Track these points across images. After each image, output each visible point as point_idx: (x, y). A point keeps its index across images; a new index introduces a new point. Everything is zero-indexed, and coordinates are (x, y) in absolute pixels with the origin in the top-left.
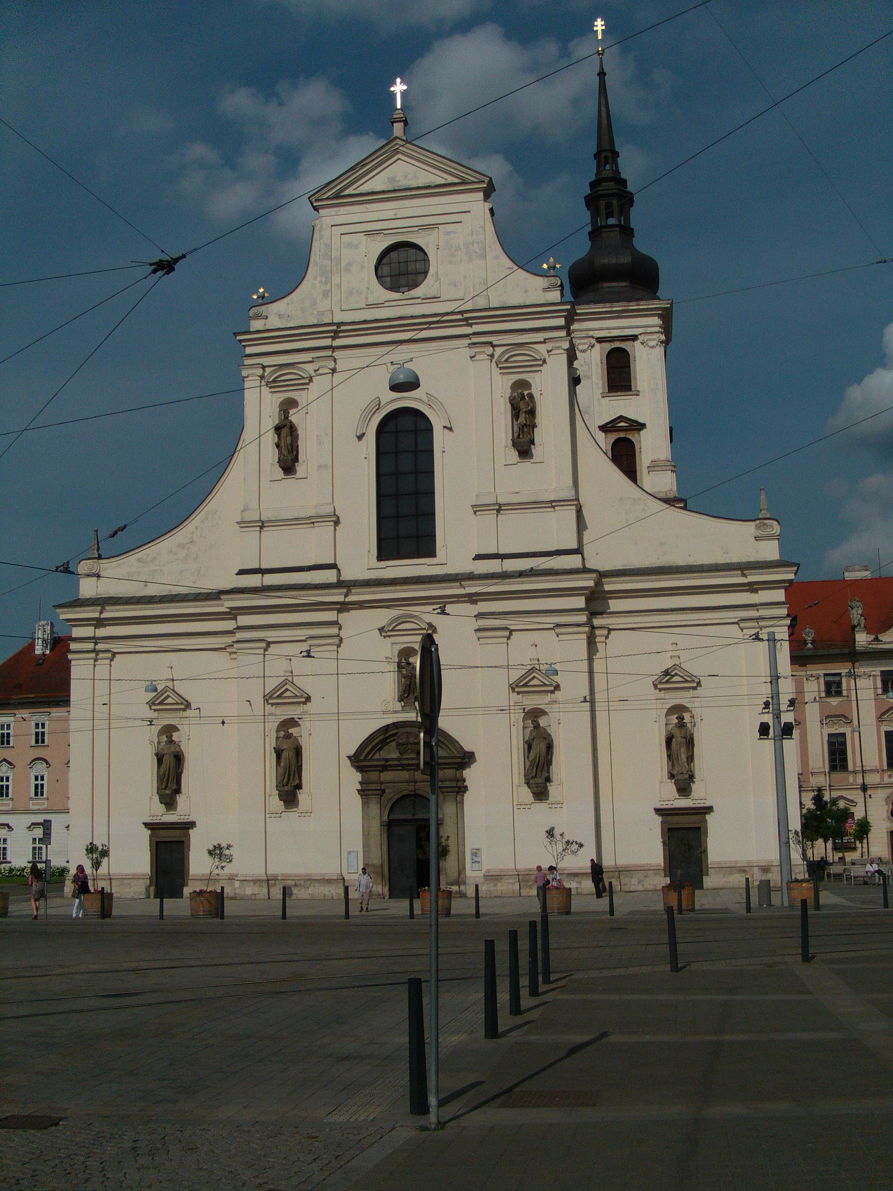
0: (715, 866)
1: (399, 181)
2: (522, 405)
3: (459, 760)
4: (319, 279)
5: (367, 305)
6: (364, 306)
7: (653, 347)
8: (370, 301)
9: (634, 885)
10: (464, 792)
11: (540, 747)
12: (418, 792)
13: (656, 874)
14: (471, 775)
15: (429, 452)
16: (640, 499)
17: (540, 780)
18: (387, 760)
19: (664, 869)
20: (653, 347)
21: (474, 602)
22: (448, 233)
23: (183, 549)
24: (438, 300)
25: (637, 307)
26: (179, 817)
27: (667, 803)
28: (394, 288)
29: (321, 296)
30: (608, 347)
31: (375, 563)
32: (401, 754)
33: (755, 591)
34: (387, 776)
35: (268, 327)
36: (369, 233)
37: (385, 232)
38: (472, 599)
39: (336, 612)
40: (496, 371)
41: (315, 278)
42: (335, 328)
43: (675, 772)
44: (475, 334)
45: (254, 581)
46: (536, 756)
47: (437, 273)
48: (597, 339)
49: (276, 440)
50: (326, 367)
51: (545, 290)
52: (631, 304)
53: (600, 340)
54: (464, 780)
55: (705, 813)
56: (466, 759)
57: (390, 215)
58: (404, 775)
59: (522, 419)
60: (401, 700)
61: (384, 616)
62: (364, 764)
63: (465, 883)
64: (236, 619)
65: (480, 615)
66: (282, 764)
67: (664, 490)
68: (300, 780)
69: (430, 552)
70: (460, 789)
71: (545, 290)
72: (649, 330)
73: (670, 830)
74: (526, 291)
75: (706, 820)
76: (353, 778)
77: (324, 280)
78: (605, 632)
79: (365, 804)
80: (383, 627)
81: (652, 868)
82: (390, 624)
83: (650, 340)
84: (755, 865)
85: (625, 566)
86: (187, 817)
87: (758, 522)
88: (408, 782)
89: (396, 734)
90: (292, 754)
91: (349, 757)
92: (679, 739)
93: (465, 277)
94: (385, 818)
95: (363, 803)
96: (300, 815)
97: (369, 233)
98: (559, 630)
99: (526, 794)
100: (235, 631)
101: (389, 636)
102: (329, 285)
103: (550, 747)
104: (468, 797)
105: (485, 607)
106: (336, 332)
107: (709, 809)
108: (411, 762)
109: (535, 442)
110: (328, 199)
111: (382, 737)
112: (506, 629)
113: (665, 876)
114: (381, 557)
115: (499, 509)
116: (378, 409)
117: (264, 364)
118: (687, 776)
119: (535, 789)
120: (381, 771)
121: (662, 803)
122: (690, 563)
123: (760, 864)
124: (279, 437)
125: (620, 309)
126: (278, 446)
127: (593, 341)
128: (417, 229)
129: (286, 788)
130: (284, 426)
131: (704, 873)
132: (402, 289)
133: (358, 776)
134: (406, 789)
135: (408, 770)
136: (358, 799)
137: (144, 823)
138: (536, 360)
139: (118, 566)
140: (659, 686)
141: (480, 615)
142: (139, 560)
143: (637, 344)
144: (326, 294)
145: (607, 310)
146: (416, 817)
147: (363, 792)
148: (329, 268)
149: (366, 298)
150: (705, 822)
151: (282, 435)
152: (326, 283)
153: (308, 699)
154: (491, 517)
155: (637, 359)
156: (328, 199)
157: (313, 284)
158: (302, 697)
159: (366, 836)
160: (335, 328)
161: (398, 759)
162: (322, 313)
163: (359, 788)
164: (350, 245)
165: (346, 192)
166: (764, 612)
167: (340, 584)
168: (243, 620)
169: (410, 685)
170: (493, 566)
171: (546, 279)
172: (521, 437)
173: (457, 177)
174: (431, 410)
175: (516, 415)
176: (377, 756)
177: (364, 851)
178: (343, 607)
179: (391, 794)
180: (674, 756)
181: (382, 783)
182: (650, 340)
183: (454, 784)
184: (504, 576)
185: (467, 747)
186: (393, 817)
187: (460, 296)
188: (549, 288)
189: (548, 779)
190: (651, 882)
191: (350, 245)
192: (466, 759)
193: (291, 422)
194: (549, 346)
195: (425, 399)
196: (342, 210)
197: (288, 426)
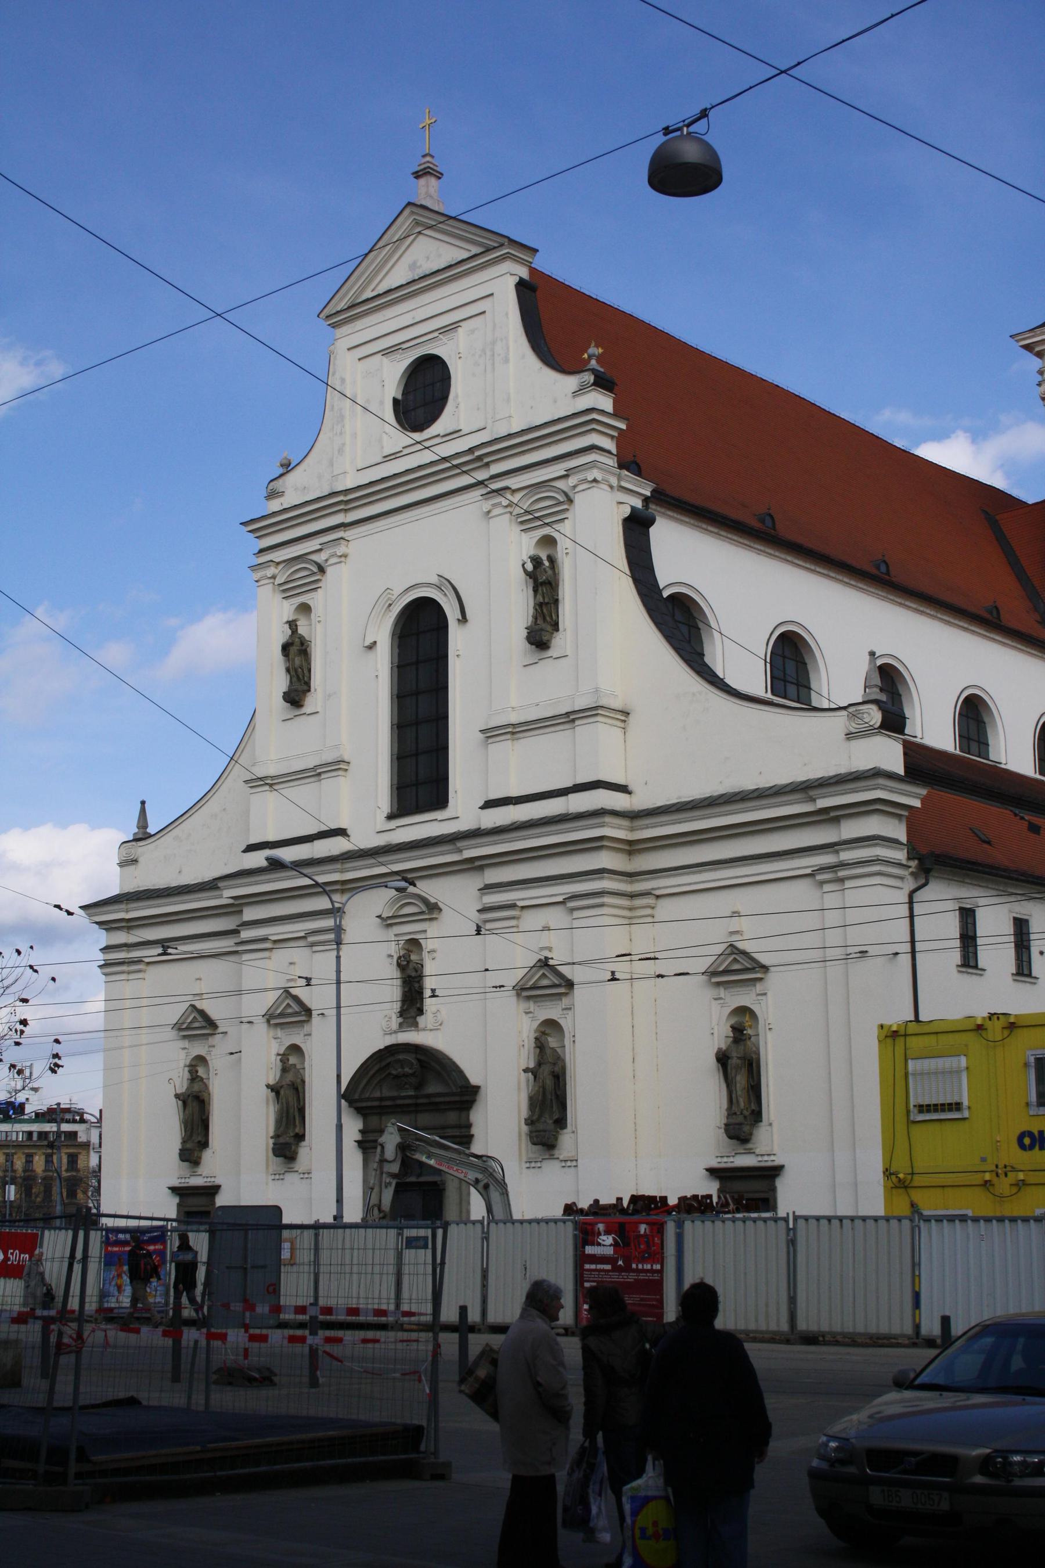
1: (421, 266)
5: (385, 457)
6: (380, 460)
21: (481, 868)
22: (473, 331)
26: (205, 1180)
27: (725, 1159)
33: (836, 820)
35: (286, 506)
36: (387, 352)
37: (404, 346)
38: (476, 865)
44: (493, 477)
45: (258, 859)
46: (538, 1091)
51: (576, 394)
54: (469, 1126)
64: (241, 912)
65: (488, 888)
71: (576, 394)
78: (649, 901)
85: (680, 798)
86: (213, 1179)
96: (302, 1176)
97: (387, 352)
98: (572, 904)
100: (239, 928)
105: (494, 876)
107: (775, 1171)
111: (376, 1068)
112: (512, 906)
116: (390, 605)
117: (277, 560)
119: (535, 1139)
128: (436, 334)
129: (281, 1140)
137: (169, 1188)
138: (560, 503)
141: (488, 888)
146: (422, 1179)
150: (773, 1190)
163: (359, 1137)
165: (369, 294)
166: (846, 856)
168: (250, 914)
169: (410, 989)
172: (538, 622)
173: (479, 244)
185: (474, 1080)
188: (582, 390)
194: (572, 481)
196: (359, 324)
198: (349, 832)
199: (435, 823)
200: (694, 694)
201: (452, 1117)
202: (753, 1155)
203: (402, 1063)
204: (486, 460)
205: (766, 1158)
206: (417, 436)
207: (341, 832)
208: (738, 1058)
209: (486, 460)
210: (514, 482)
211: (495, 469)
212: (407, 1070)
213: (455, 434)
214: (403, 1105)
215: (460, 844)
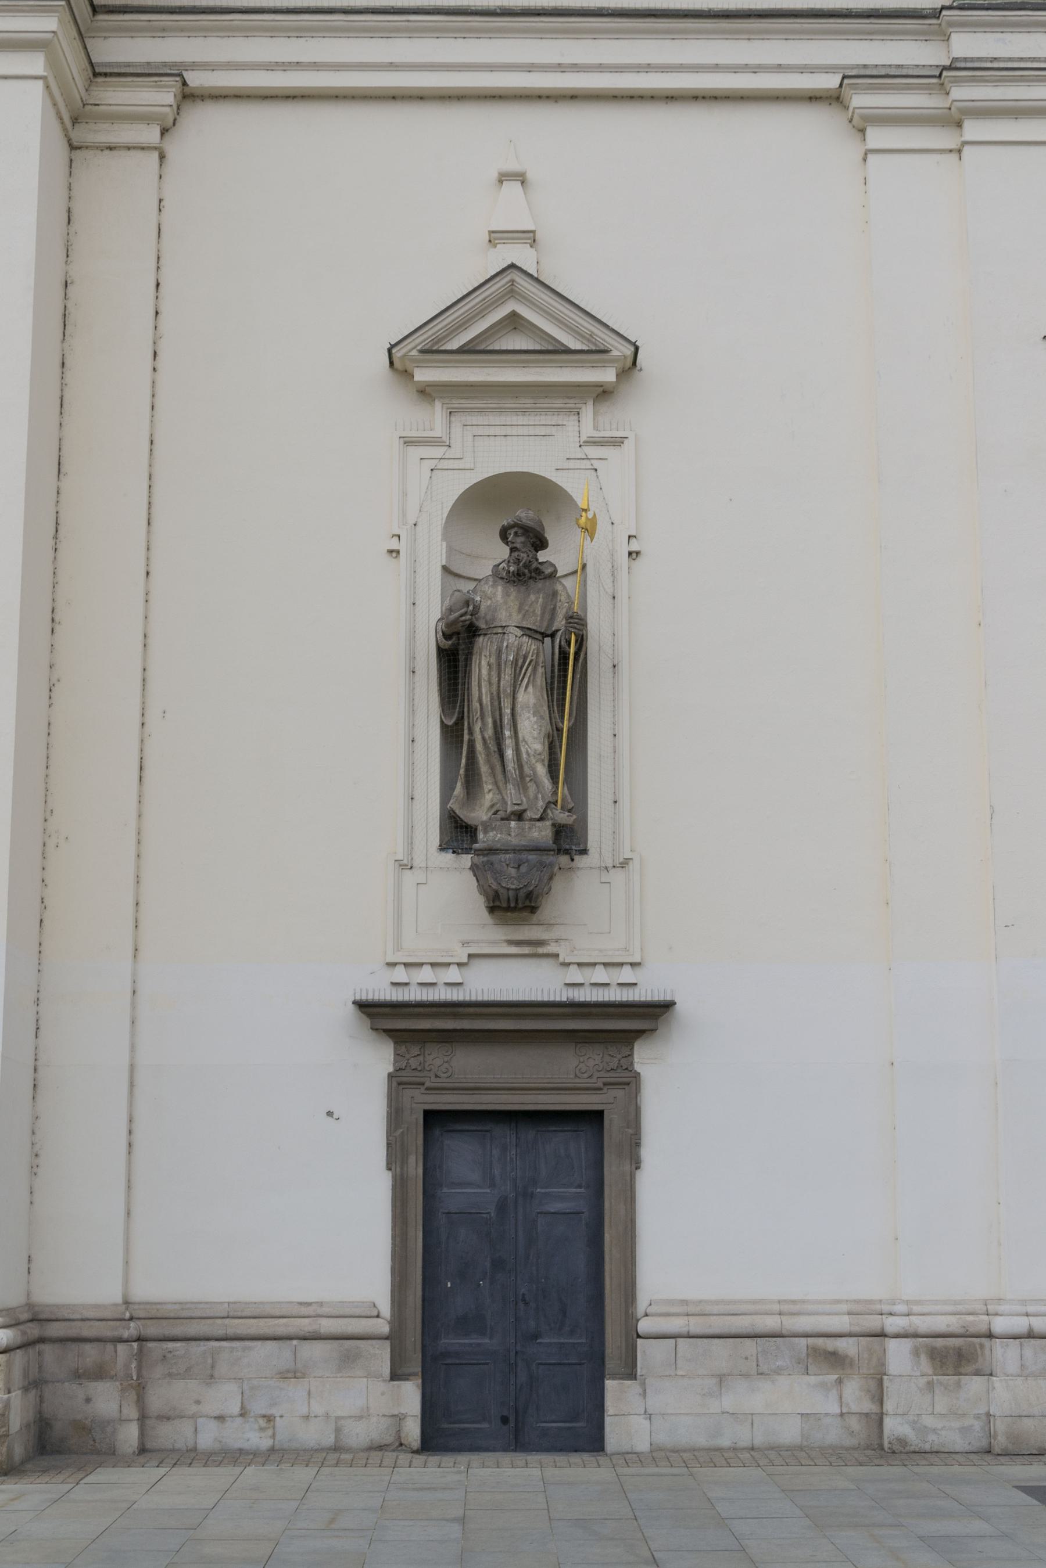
0: (676, 1325)
9: (220, 1418)
13: (347, 1361)
19: (395, 1337)
27: (426, 974)
43: (479, 814)
55: (630, 1037)
73: (433, 1118)
75: (637, 1076)
81: (327, 1326)
84: (893, 1324)
92: (513, 638)
113: (395, 1376)
118: (542, 833)
121: (400, 975)
123: (922, 1324)
131: (610, 1365)
140: (423, 375)
180: (481, 731)
190: (317, 1408)
202: (546, 965)
205: (600, 975)
208: (529, 632)
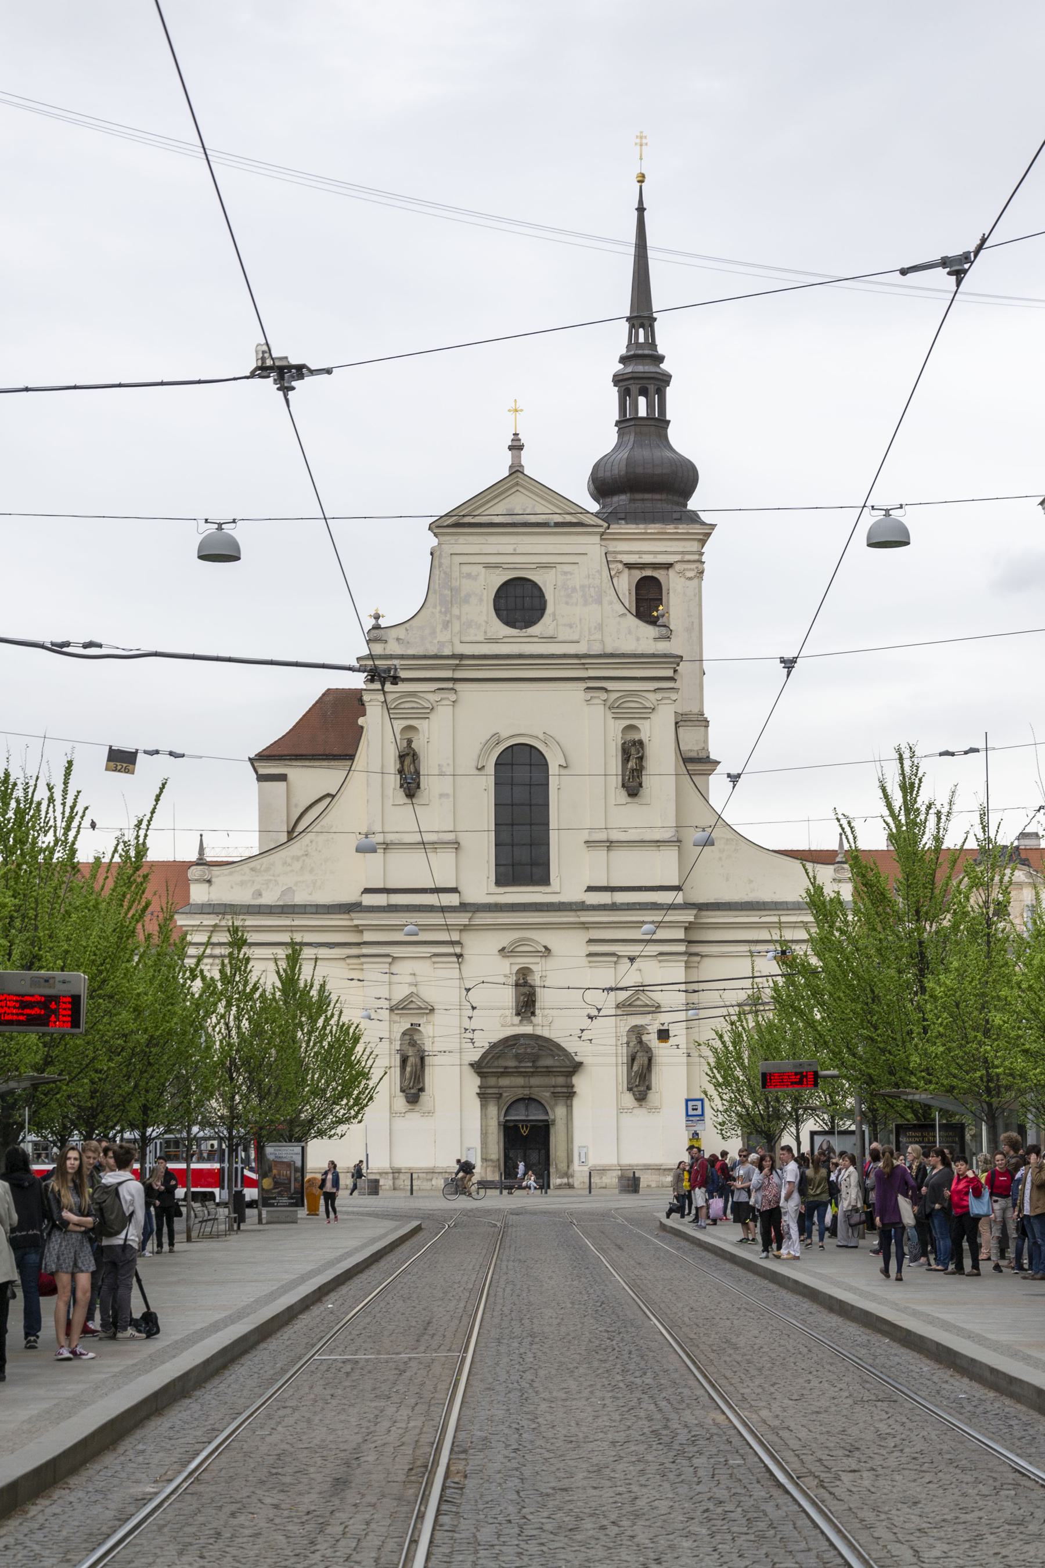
2: (633, 751)
3: (571, 1070)
4: (438, 608)
6: (481, 639)
7: (690, 579)
8: (489, 635)
10: (573, 1096)
11: (641, 1060)
12: (533, 1096)
14: (581, 1083)
15: (544, 785)
16: (732, 840)
17: (642, 1088)
18: (506, 1068)
20: (690, 579)
22: (565, 573)
23: (298, 861)
24: (555, 640)
25: (675, 531)
28: (509, 623)
29: (441, 626)
30: (638, 575)
31: (494, 889)
32: (520, 1062)
34: (505, 1081)
35: (388, 652)
36: (488, 566)
37: (503, 565)
38: (585, 926)
39: (458, 933)
40: (610, 715)
41: (435, 607)
42: (457, 662)
47: (554, 614)
48: (625, 564)
49: (398, 766)
50: (448, 699)
52: (668, 527)
53: (629, 566)
54: (573, 1086)
56: (576, 1067)
57: (509, 549)
58: (520, 1081)
59: (631, 764)
60: (518, 1014)
61: (506, 939)
62: (485, 1070)
63: (572, 1176)
65: (590, 941)
66: (408, 1069)
67: (695, 749)
68: (424, 1084)
69: (545, 880)
70: (569, 1094)
72: (688, 557)
74: (638, 639)
76: (473, 1083)
77: (443, 610)
78: (698, 959)
79: (484, 1107)
80: (503, 949)
82: (511, 946)
83: (687, 570)
87: (836, 865)
88: (523, 1087)
89: (515, 1044)
90: (418, 1060)
91: (471, 1065)
93: (580, 620)
94: (502, 1119)
95: (481, 1105)
97: (488, 566)
98: (660, 958)
99: (629, 1099)
101: (508, 956)
102: (448, 615)
103: (650, 1060)
104: (576, 1102)
106: (457, 665)
108: (528, 1070)
109: (643, 785)
110: (448, 526)
112: (613, 954)
114: (499, 883)
115: (610, 845)
120: (498, 1077)
122: (775, 900)
124: (402, 763)
125: (656, 531)
126: (401, 772)
127: (620, 566)
128: (534, 566)
130: (408, 754)
132: (518, 624)
133: (477, 1081)
134: (521, 1093)
135: (524, 1076)
136: (477, 1102)
139: (231, 874)
141: (590, 941)
142: (252, 869)
143: (671, 572)
144: (446, 625)
145: (639, 531)
147: (483, 1096)
148: (449, 599)
149: (485, 632)
151: (406, 763)
152: (445, 613)
153: (432, 1010)
154: (601, 854)
155: (671, 591)
156: (448, 526)
157: (433, 613)
158: (427, 1009)
159: (484, 1134)
160: (457, 662)
161: (516, 1067)
162: (441, 644)
163: (478, 1091)
164: (469, 576)
167: (464, 907)
170: (605, 898)
171: (657, 629)
174: (546, 749)
175: (626, 759)
176: (496, 1064)
177: (482, 1148)
178: (465, 928)
179: (509, 1096)
181: (500, 1087)
182: (687, 570)
183: (564, 1090)
184: (614, 907)
186: (508, 1118)
187: (575, 638)
189: (649, 1088)
191: (469, 576)
192: (576, 1067)
193: (414, 750)
194: (659, 696)
195: (541, 736)
197: (411, 754)
198: (459, 889)
199: (541, 894)
200: (727, 840)
201: (561, 1080)
203: (527, 1046)
204: (587, 666)
206: (514, 632)
207: (455, 890)
209: (587, 666)
210: (609, 685)
211: (592, 673)
212: (529, 1050)
213: (551, 639)
214: (525, 1072)
215: (579, 913)
